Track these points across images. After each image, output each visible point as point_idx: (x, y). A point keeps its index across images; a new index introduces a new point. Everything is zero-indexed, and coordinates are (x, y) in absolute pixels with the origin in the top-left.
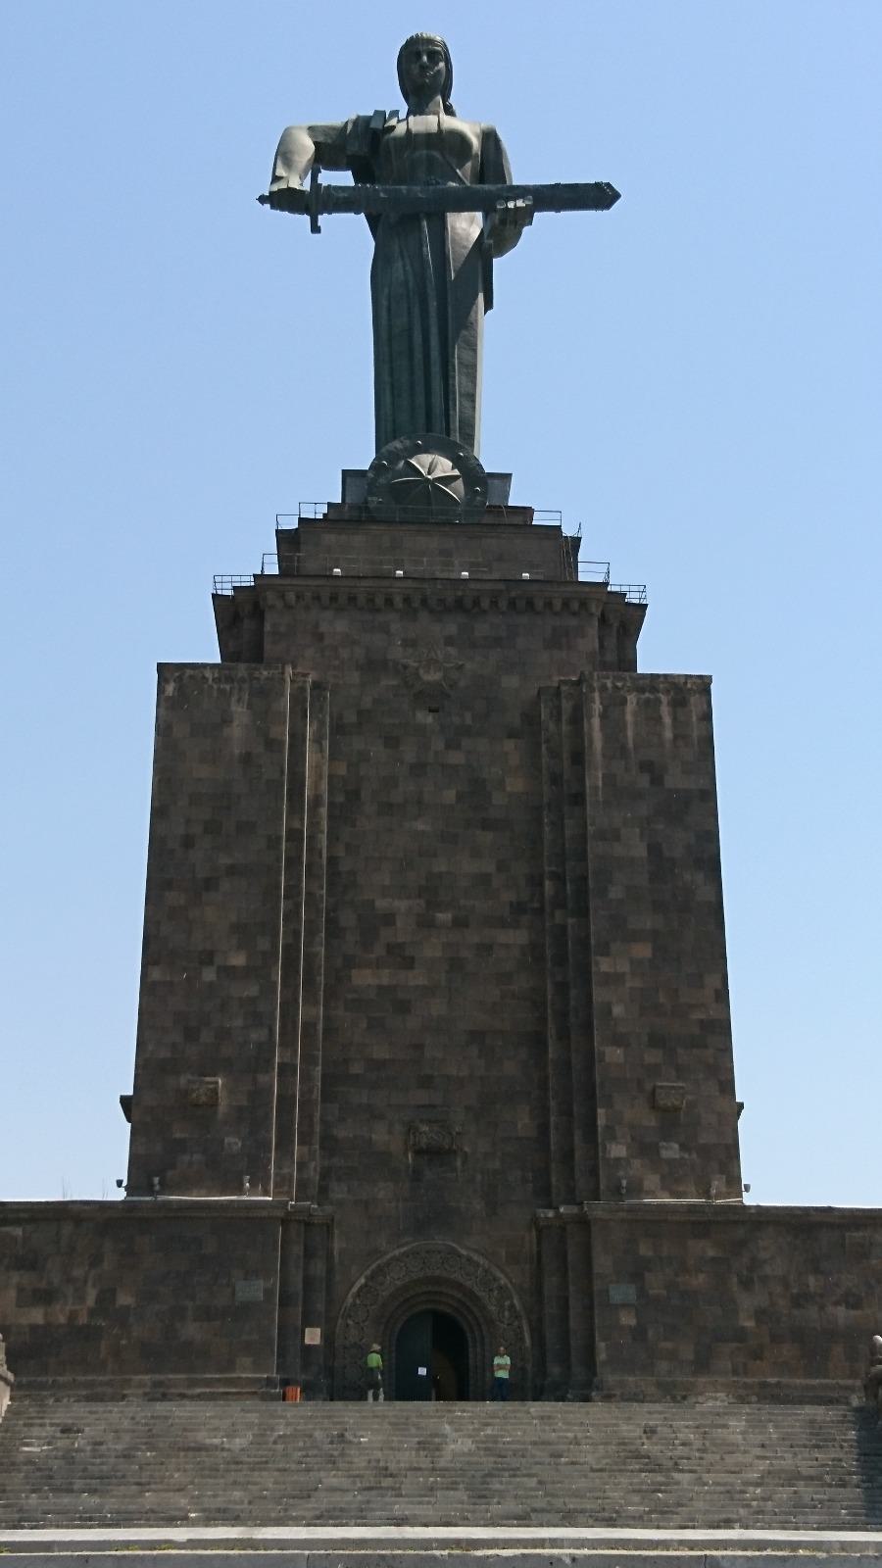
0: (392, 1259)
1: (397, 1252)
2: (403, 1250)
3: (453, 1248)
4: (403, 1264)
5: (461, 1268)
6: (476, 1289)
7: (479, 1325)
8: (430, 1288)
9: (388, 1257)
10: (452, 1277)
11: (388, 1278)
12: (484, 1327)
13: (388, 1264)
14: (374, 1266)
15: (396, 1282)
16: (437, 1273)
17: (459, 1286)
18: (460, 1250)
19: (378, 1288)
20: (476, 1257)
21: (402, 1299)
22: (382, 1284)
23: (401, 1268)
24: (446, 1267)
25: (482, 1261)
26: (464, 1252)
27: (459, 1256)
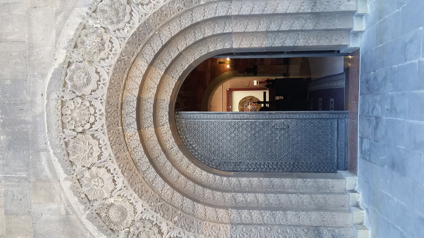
0: (77, 193)
1: (67, 185)
2: (61, 174)
3: (54, 74)
4: (87, 174)
5: (91, 62)
6: (128, 32)
7: (194, 26)
8: (131, 119)
9: (74, 200)
10: (106, 78)
11: (112, 200)
12: (198, 17)
13: (87, 200)
14: (91, 227)
15: (119, 187)
16: (101, 107)
17: (124, 67)
18: (56, 65)
19: (129, 219)
20: (70, 32)
21: (152, 173)
22: (123, 214)
23: (93, 177)
24: (87, 90)
25: (75, 21)
26: (61, 57)
27: (70, 64)
